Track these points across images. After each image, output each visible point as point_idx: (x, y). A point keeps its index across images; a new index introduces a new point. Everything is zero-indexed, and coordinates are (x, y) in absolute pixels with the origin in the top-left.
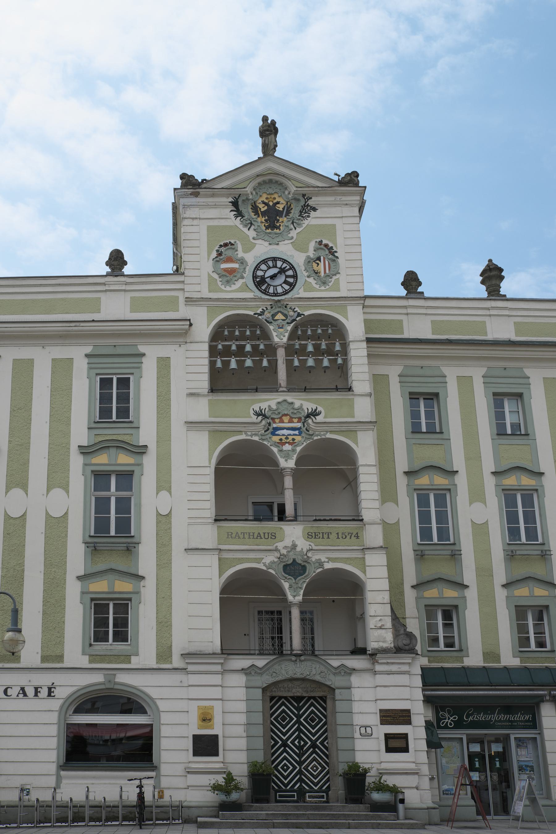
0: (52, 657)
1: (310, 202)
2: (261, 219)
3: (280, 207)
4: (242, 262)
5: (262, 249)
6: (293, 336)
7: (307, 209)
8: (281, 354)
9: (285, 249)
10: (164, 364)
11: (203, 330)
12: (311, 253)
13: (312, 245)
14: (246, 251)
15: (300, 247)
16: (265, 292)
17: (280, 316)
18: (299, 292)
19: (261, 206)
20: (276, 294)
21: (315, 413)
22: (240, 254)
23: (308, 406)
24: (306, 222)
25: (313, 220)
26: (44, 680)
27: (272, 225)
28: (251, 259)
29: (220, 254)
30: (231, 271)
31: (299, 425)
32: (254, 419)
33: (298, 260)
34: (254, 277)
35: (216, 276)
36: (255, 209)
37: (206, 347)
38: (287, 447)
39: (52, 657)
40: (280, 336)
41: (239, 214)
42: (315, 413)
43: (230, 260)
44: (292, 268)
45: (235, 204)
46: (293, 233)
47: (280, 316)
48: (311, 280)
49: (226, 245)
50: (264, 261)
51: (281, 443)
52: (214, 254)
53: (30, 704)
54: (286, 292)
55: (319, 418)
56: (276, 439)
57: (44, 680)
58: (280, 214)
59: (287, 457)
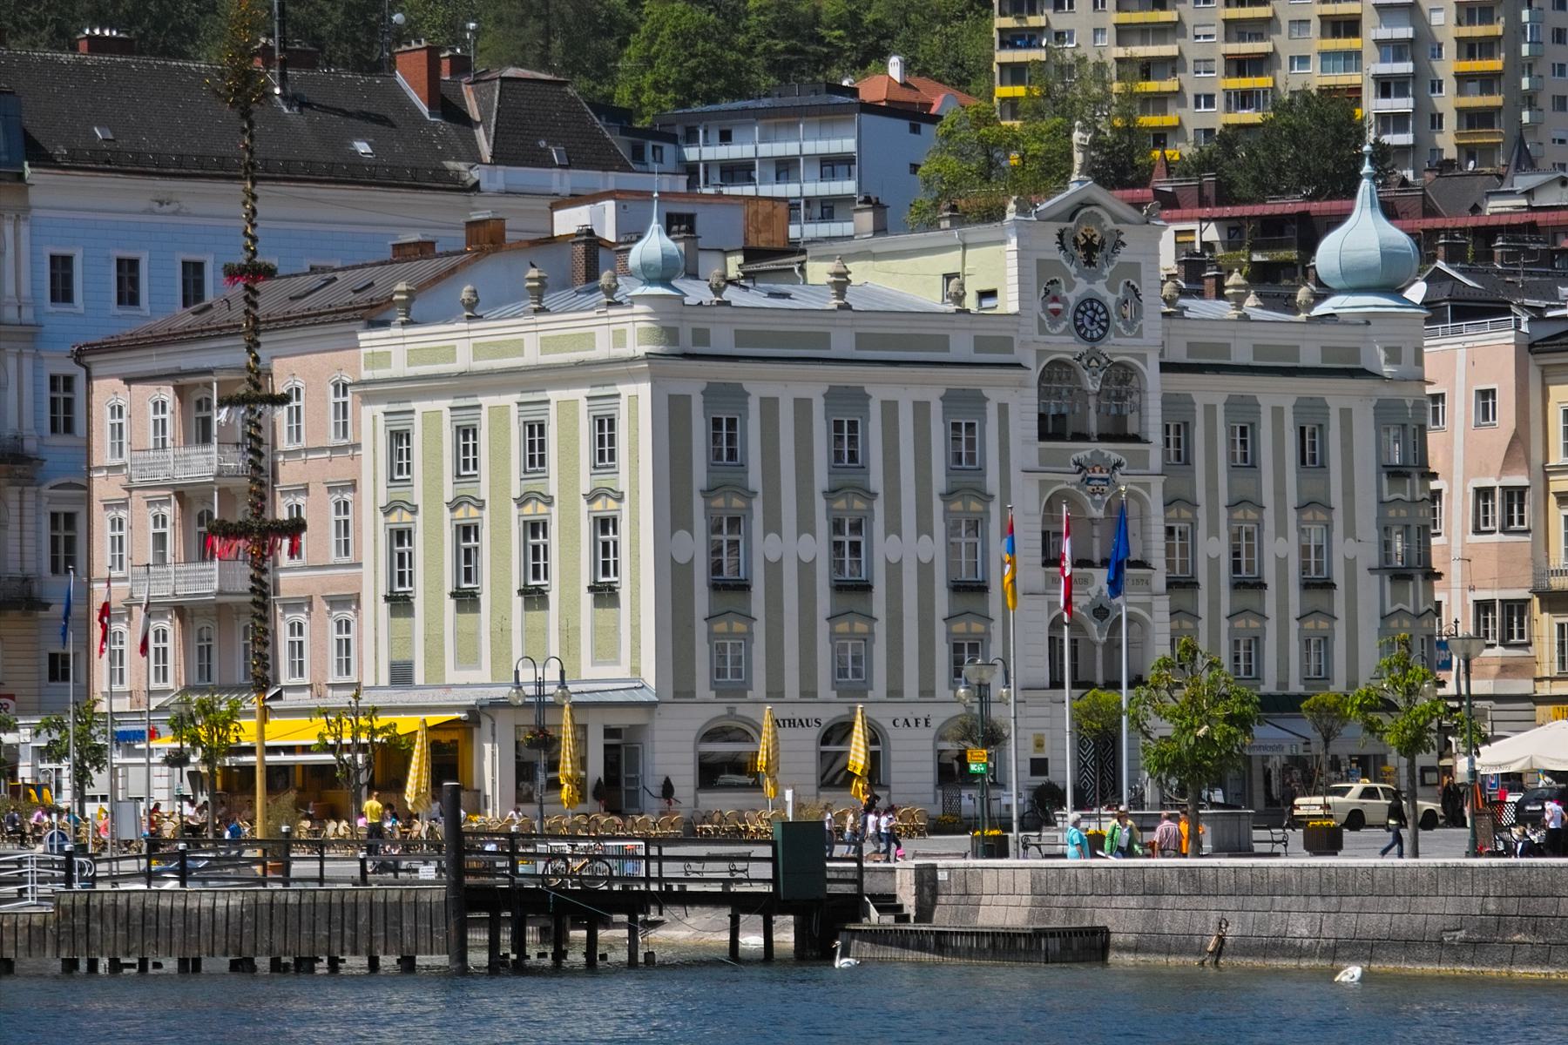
0: (927, 691)
1: (1122, 238)
2: (1081, 254)
3: (1096, 240)
4: (1065, 302)
5: (1082, 287)
6: (1105, 381)
7: (1119, 244)
8: (1092, 401)
9: (1100, 288)
10: (1003, 409)
11: (1034, 375)
12: (1121, 295)
13: (1122, 285)
14: (1069, 289)
15: (1112, 287)
16: (1083, 336)
17: (1094, 363)
18: (1112, 338)
19: (1081, 238)
20: (1092, 340)
21: (1119, 464)
22: (1064, 293)
23: (1115, 457)
24: (1117, 259)
25: (1123, 256)
26: (921, 711)
27: (1089, 263)
28: (1072, 297)
29: (1047, 293)
30: (1056, 312)
31: (1106, 475)
32: (1074, 468)
33: (1111, 300)
34: (1076, 319)
35: (1044, 317)
36: (1076, 240)
37: (1035, 392)
38: (1098, 497)
39: (927, 691)
40: (1092, 384)
41: (1063, 247)
42: (1119, 464)
43: (1055, 299)
44: (1105, 311)
45: (1060, 236)
46: (1107, 271)
47: (1094, 363)
48: (1120, 325)
49: (1052, 282)
50: (1083, 303)
51: (1094, 493)
52: (1043, 292)
53: (912, 732)
54: (1100, 337)
55: (1123, 469)
56: (1089, 488)
57: (921, 711)
58: (1096, 248)
59: (1097, 504)
